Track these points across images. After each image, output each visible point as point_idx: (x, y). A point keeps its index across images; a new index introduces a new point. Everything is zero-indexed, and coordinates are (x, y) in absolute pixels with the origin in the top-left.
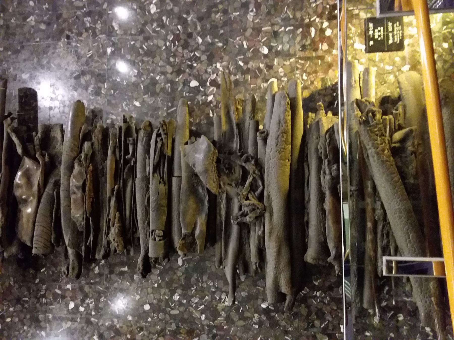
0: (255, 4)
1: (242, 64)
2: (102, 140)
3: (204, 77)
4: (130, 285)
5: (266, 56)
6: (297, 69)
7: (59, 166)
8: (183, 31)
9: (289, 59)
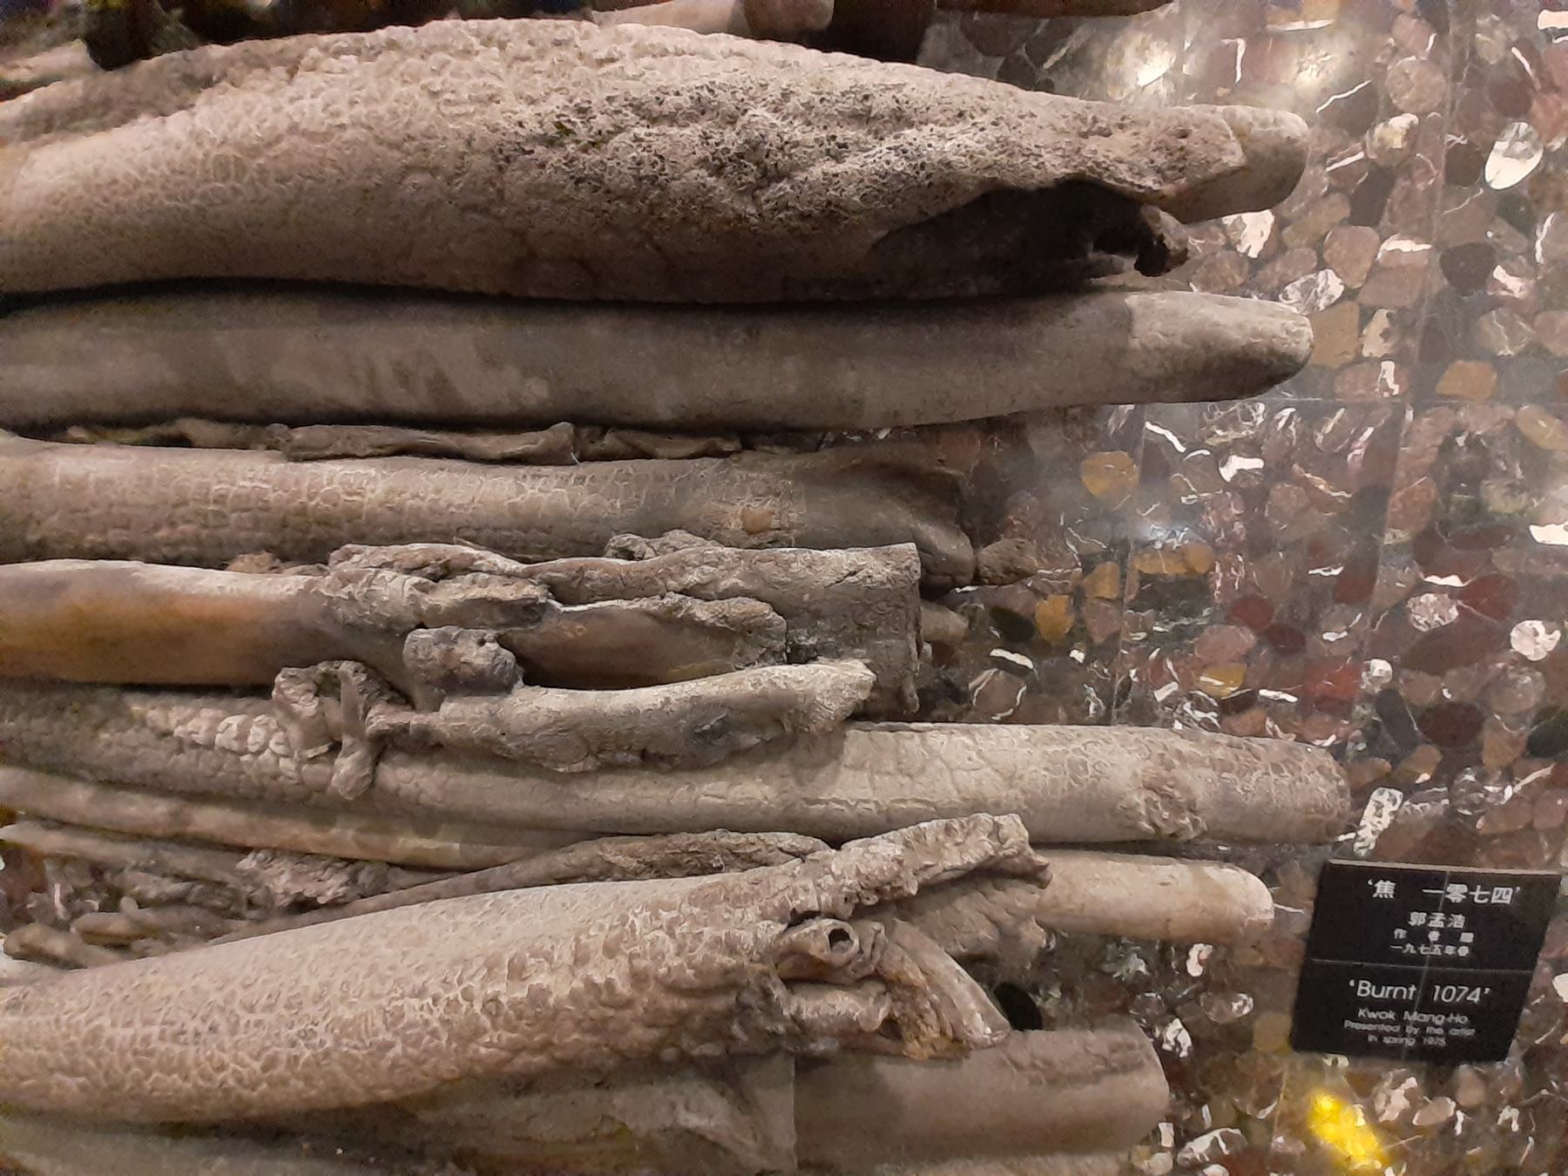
9: (1399, 357)
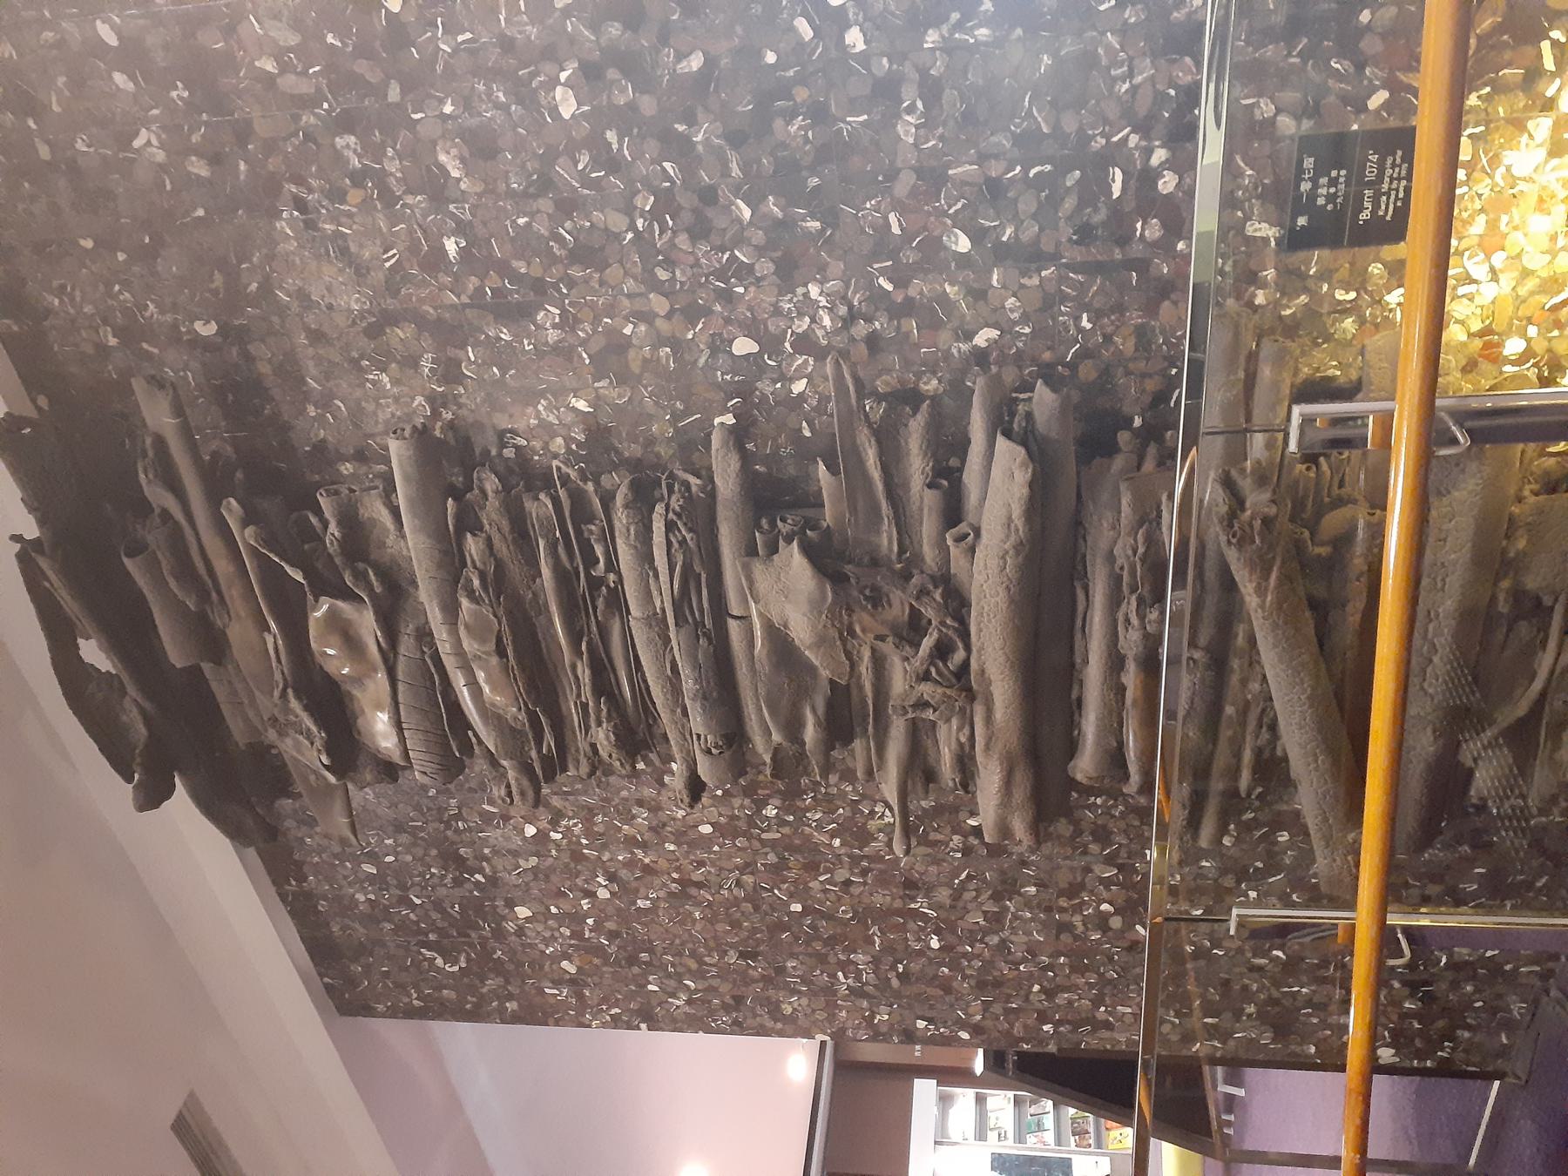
0: (921, 85)
1: (889, 287)
2: (512, 531)
3: (772, 328)
4: (659, 793)
5: (963, 260)
6: (1064, 298)
7: (411, 590)
8: (684, 181)
9: (1039, 271)
